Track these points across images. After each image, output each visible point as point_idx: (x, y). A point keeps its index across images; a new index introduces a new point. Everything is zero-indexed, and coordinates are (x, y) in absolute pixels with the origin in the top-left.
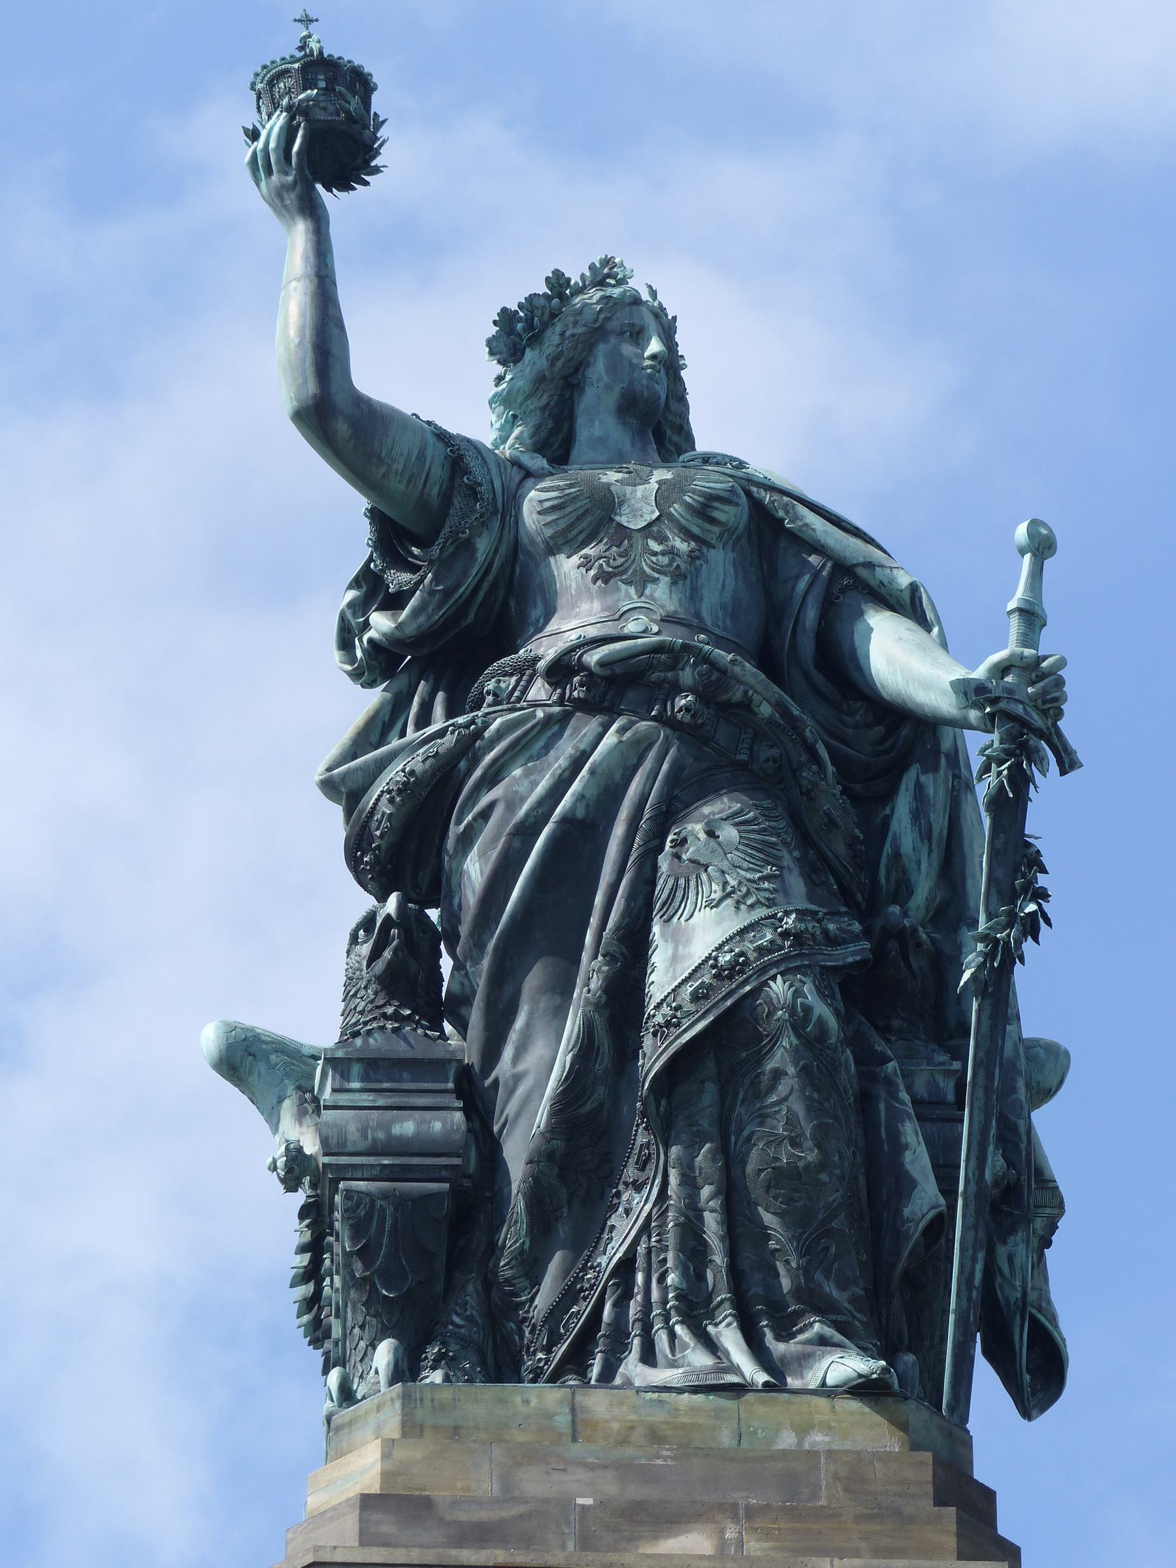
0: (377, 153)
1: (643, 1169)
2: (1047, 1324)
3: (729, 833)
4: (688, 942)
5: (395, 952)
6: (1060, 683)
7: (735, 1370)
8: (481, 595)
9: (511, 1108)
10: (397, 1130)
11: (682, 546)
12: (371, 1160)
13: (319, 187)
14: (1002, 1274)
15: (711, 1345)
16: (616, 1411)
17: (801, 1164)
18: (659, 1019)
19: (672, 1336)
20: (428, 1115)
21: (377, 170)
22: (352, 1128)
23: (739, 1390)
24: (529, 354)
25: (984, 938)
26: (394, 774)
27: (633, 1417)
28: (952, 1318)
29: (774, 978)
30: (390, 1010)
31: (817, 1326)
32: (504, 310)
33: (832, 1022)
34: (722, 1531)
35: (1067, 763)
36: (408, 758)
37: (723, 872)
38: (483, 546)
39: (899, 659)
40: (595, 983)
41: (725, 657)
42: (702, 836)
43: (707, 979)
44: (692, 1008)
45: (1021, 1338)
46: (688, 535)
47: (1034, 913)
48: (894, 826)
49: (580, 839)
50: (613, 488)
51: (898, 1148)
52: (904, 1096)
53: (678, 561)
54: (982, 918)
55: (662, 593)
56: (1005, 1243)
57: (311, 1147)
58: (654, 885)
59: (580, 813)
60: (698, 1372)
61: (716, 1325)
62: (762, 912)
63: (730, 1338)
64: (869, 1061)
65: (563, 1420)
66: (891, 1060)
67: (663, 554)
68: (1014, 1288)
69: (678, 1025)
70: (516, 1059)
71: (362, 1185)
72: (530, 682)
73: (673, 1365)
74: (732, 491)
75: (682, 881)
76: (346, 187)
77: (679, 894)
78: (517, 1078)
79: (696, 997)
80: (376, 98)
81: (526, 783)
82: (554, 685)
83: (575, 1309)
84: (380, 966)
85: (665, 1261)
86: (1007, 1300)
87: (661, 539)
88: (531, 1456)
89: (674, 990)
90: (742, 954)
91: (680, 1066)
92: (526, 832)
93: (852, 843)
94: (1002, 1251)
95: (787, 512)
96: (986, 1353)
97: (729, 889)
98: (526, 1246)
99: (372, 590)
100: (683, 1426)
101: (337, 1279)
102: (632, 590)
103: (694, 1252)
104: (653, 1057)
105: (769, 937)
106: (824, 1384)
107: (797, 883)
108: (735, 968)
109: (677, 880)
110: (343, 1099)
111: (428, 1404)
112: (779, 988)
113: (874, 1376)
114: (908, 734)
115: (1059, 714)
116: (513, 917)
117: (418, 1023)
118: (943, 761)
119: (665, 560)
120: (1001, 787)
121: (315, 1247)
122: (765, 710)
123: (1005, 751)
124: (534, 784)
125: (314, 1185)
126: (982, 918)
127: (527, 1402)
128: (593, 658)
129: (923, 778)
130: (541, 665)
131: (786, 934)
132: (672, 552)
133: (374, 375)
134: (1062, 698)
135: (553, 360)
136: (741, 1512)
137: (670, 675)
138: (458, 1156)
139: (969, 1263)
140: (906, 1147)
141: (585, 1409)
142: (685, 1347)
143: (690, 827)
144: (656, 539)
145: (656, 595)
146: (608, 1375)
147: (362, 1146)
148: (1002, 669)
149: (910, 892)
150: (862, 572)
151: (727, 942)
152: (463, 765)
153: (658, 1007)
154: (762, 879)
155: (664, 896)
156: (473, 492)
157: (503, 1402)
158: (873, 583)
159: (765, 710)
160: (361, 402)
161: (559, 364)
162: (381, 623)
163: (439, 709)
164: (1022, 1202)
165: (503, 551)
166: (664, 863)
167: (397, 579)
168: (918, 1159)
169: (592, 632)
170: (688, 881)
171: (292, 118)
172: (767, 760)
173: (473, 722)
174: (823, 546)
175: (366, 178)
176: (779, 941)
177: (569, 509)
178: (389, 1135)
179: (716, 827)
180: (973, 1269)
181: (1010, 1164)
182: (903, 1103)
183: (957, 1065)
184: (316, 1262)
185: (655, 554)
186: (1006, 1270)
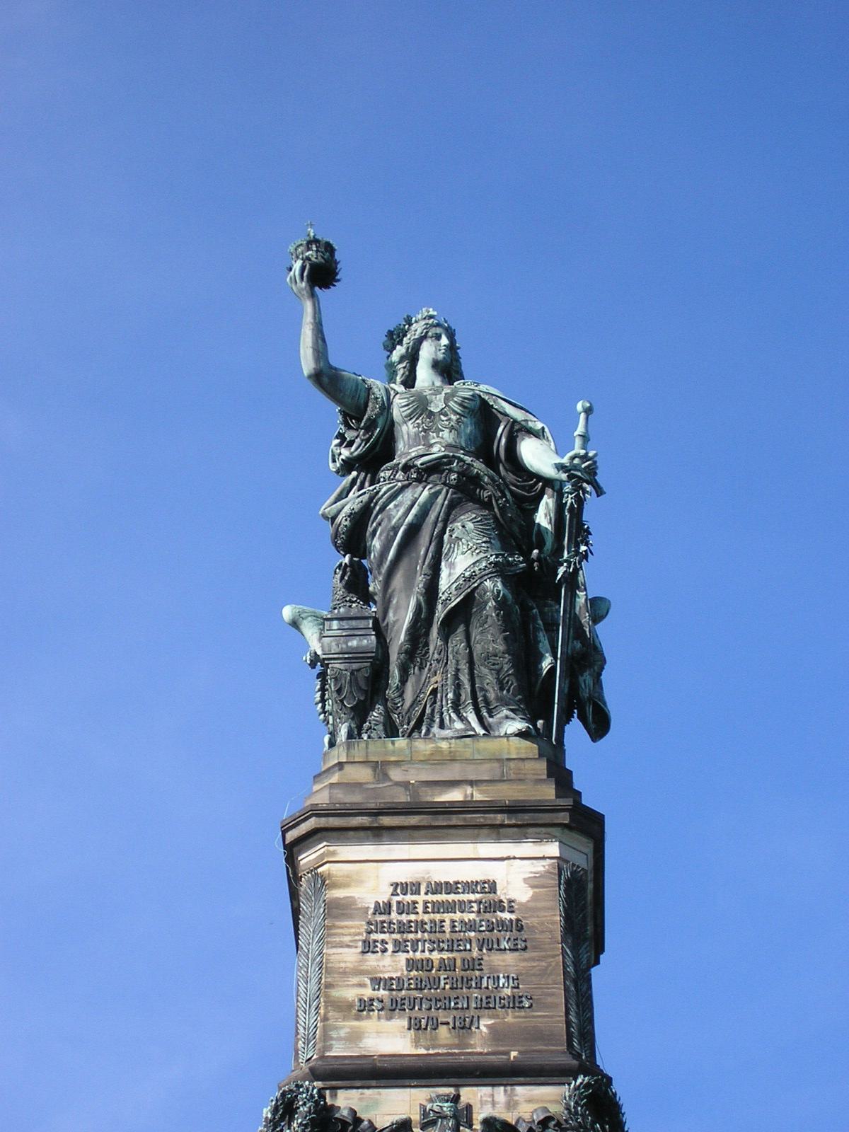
0: (337, 274)
1: (440, 654)
2: (602, 705)
3: (470, 526)
4: (454, 568)
5: (349, 577)
6: (595, 462)
7: (473, 730)
8: (381, 439)
9: (393, 635)
10: (350, 644)
11: (454, 417)
12: (341, 656)
13: (317, 289)
15: (462, 718)
17: (497, 651)
18: (443, 598)
19: (450, 716)
20: (362, 637)
21: (338, 280)
22: (334, 644)
25: (566, 561)
26: (347, 510)
29: (486, 580)
30: (348, 599)
31: (505, 711)
32: (389, 331)
33: (510, 596)
34: (466, 791)
35: (599, 491)
36: (353, 502)
37: (468, 541)
40: (421, 586)
41: (468, 459)
42: (460, 528)
43: (461, 582)
44: (455, 593)
45: (590, 710)
46: (456, 413)
47: (586, 551)
49: (413, 531)
50: (428, 397)
52: (540, 622)
53: (452, 423)
54: (566, 552)
55: (447, 436)
56: (582, 676)
57: (319, 652)
58: (443, 546)
59: (415, 522)
60: (457, 730)
61: (466, 712)
62: (482, 555)
63: (472, 718)
64: (525, 609)
66: (534, 609)
67: (447, 420)
69: (450, 600)
72: (397, 472)
73: (451, 729)
74: (472, 396)
75: (453, 545)
76: (327, 287)
77: (451, 551)
79: (456, 589)
80: (336, 253)
81: (395, 511)
82: (405, 473)
83: (417, 709)
84: (344, 582)
85: (447, 690)
87: (446, 415)
89: (449, 587)
90: (474, 572)
92: (395, 529)
93: (521, 527)
95: (495, 402)
96: (578, 717)
97: (469, 547)
101: (330, 701)
102: (434, 434)
103: (458, 687)
104: (440, 613)
105: (484, 564)
106: (506, 734)
107: (496, 542)
110: (330, 633)
112: (488, 584)
113: (524, 730)
115: (595, 474)
117: (359, 603)
119: (447, 423)
120: (572, 502)
121: (323, 689)
122: (486, 479)
123: (573, 489)
124: (398, 511)
125: (322, 666)
126: (566, 552)
128: (418, 462)
130: (401, 465)
131: (490, 564)
132: (449, 420)
134: (596, 468)
137: (448, 467)
140: (540, 641)
142: (454, 721)
143: (456, 524)
144: (444, 415)
145: (444, 437)
146: (428, 731)
147: (337, 651)
148: (573, 458)
149: (545, 544)
151: (468, 567)
153: (443, 594)
154: (482, 543)
155: (446, 551)
159: (486, 479)
163: (367, 484)
164: (585, 658)
165: (388, 422)
166: (446, 537)
167: (349, 435)
168: (544, 644)
169: (421, 453)
170: (454, 545)
171: (303, 263)
173: (375, 488)
175: (335, 284)
176: (488, 566)
177: (411, 406)
179: (467, 526)
181: (583, 645)
182: (539, 625)
183: (557, 607)
184: (323, 696)
185: (443, 421)
186: (583, 686)
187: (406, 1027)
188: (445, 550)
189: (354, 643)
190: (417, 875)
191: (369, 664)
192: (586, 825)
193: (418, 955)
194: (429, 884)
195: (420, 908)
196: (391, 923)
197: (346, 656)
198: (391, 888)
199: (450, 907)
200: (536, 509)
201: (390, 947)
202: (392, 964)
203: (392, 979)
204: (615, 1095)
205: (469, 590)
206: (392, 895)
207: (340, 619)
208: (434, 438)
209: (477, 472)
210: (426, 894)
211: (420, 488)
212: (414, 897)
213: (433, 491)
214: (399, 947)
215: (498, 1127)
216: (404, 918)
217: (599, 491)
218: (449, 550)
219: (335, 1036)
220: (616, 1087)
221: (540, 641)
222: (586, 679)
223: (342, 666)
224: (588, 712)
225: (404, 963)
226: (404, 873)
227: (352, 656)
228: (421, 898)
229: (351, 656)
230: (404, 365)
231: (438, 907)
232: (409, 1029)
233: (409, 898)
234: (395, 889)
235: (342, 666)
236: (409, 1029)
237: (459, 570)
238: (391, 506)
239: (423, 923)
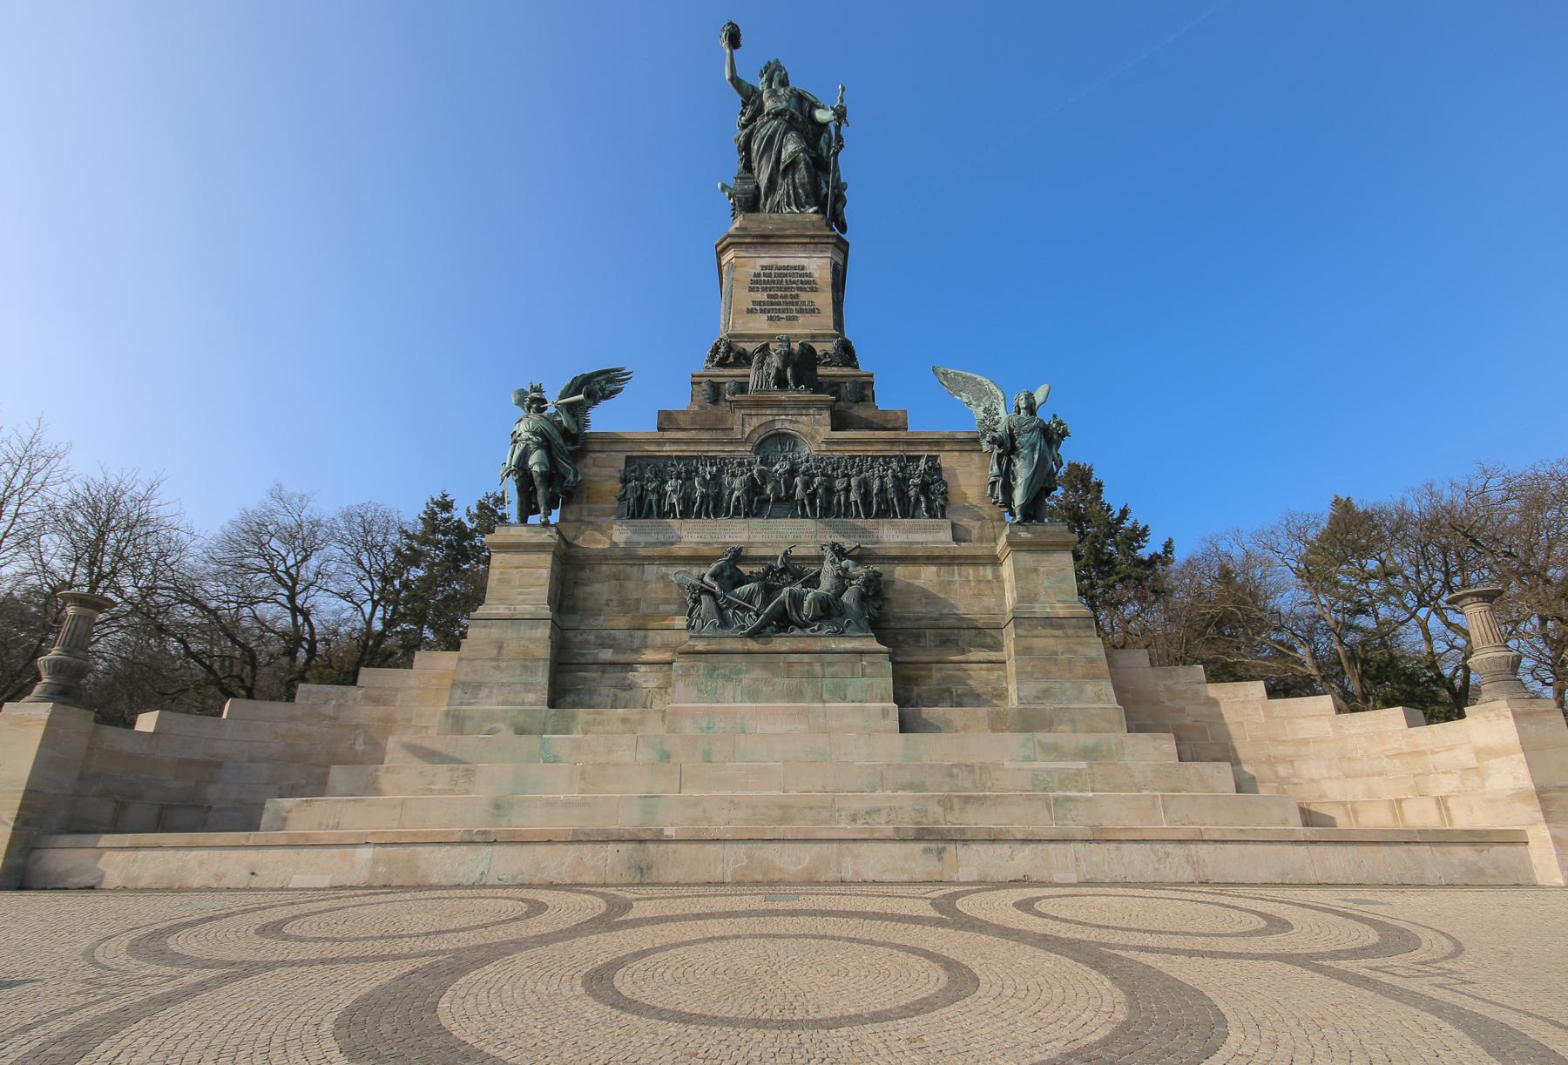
39: (822, 115)
91: (786, 168)
104: (782, 167)
114: (824, 126)
164: (839, 198)
192: (842, 246)
202: (763, 296)
214: (764, 289)
222: (839, 206)
226: (767, 262)
227: (745, 192)
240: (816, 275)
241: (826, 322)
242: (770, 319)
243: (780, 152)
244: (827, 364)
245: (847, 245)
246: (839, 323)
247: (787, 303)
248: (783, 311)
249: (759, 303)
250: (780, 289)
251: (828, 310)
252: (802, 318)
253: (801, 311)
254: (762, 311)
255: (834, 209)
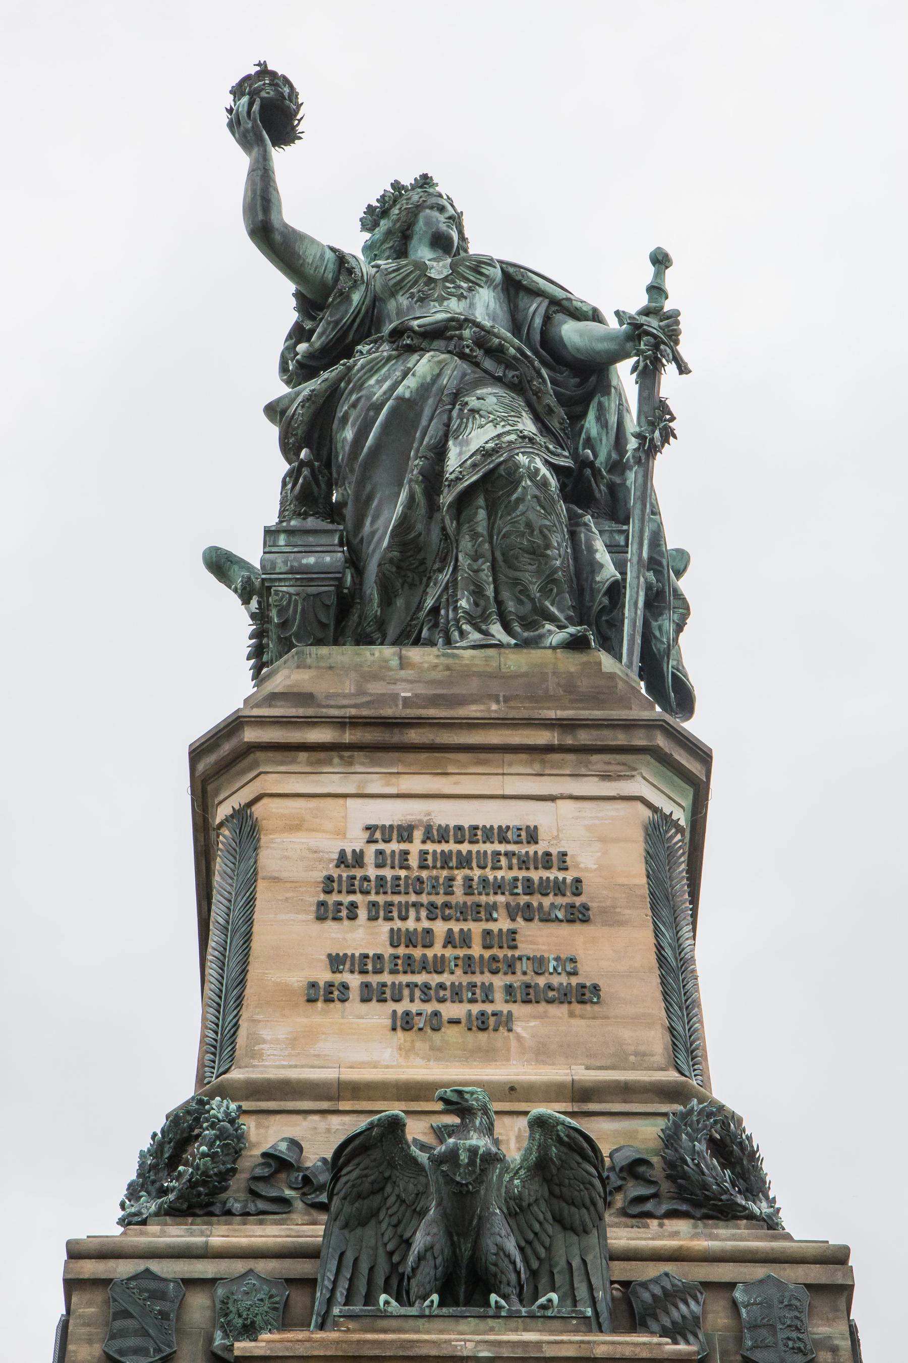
8: (356, 324)
10: (304, 561)
12: (290, 576)
14: (655, 637)
16: (426, 658)
23: (500, 646)
24: (383, 222)
27: (436, 661)
28: (626, 621)
29: (517, 454)
32: (369, 206)
35: (683, 369)
38: (356, 297)
48: (587, 425)
51: (592, 551)
59: (407, 395)
65: (395, 663)
68: (663, 643)
70: (372, 523)
71: (284, 589)
75: (465, 420)
78: (373, 533)
86: (659, 650)
87: (453, 282)
88: (375, 677)
91: (464, 500)
92: (378, 408)
94: (654, 624)
98: (379, 613)
99: (299, 333)
100: (467, 665)
104: (447, 498)
108: (495, 451)
109: (462, 420)
111: (313, 656)
116: (370, 448)
118: (613, 390)
124: (381, 387)
127: (373, 654)
129: (602, 399)
133: (294, 213)
135: (395, 223)
136: (501, 699)
137: (457, 332)
138: (339, 573)
139: (635, 595)
141: (408, 658)
147: (284, 569)
150: (565, 303)
152: (343, 385)
153: (451, 473)
156: (350, 271)
157: (359, 654)
158: (572, 309)
160: (286, 226)
161: (398, 225)
162: (302, 347)
164: (663, 601)
168: (603, 556)
170: (468, 419)
172: (513, 377)
174: (543, 292)
178: (301, 564)
180: (637, 598)
185: (449, 288)
186: (657, 633)
187: (390, 1027)
188: (455, 424)
189: (311, 560)
190: (410, 818)
191: (332, 588)
193: (411, 924)
194: (428, 829)
195: (414, 861)
196: (366, 879)
197: (298, 576)
198: (366, 835)
199: (465, 861)
200: (584, 414)
201: (362, 913)
202: (366, 937)
203: (366, 956)
204: (749, 1138)
205: (491, 466)
206: (368, 842)
207: (290, 532)
208: (435, 307)
209: (500, 344)
210: (424, 842)
211: (416, 357)
212: (404, 846)
213: (436, 359)
215: (562, 1135)
216: (388, 873)
217: (683, 369)
218: (460, 426)
219: (268, 1038)
220: (749, 1127)
221: (597, 551)
223: (292, 590)
224: (665, 669)
225: (385, 937)
227: (304, 576)
228: (415, 847)
229: (305, 576)
230: (391, 244)
231: (445, 860)
232: (394, 1029)
233: (395, 846)
234: (372, 835)
235: (292, 590)
236: (394, 1029)
237: (473, 447)
238: (372, 382)
239: (419, 880)
240: (586, 861)
241: (633, 1035)
242: (405, 1023)
243: (440, 453)
244: (638, 1213)
245: (704, 756)
246: (685, 1045)
247: (469, 965)
248: (456, 995)
249: (362, 964)
250: (433, 912)
251: (636, 990)
252: (529, 1022)
253: (528, 995)
254: (368, 994)
255: (647, 636)
